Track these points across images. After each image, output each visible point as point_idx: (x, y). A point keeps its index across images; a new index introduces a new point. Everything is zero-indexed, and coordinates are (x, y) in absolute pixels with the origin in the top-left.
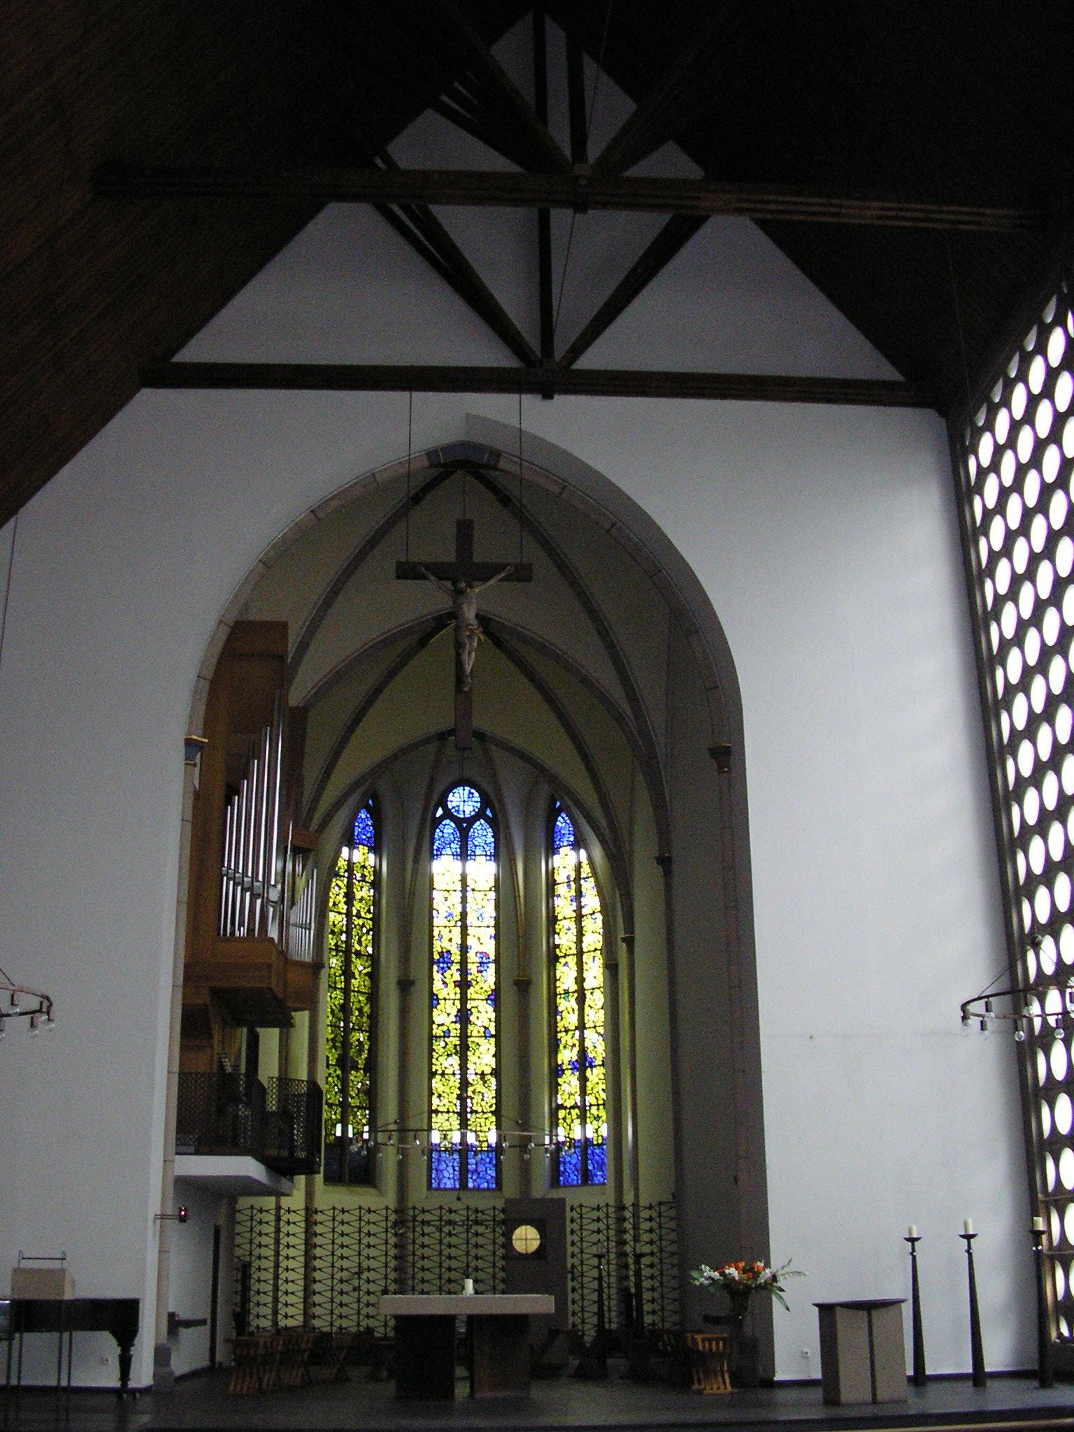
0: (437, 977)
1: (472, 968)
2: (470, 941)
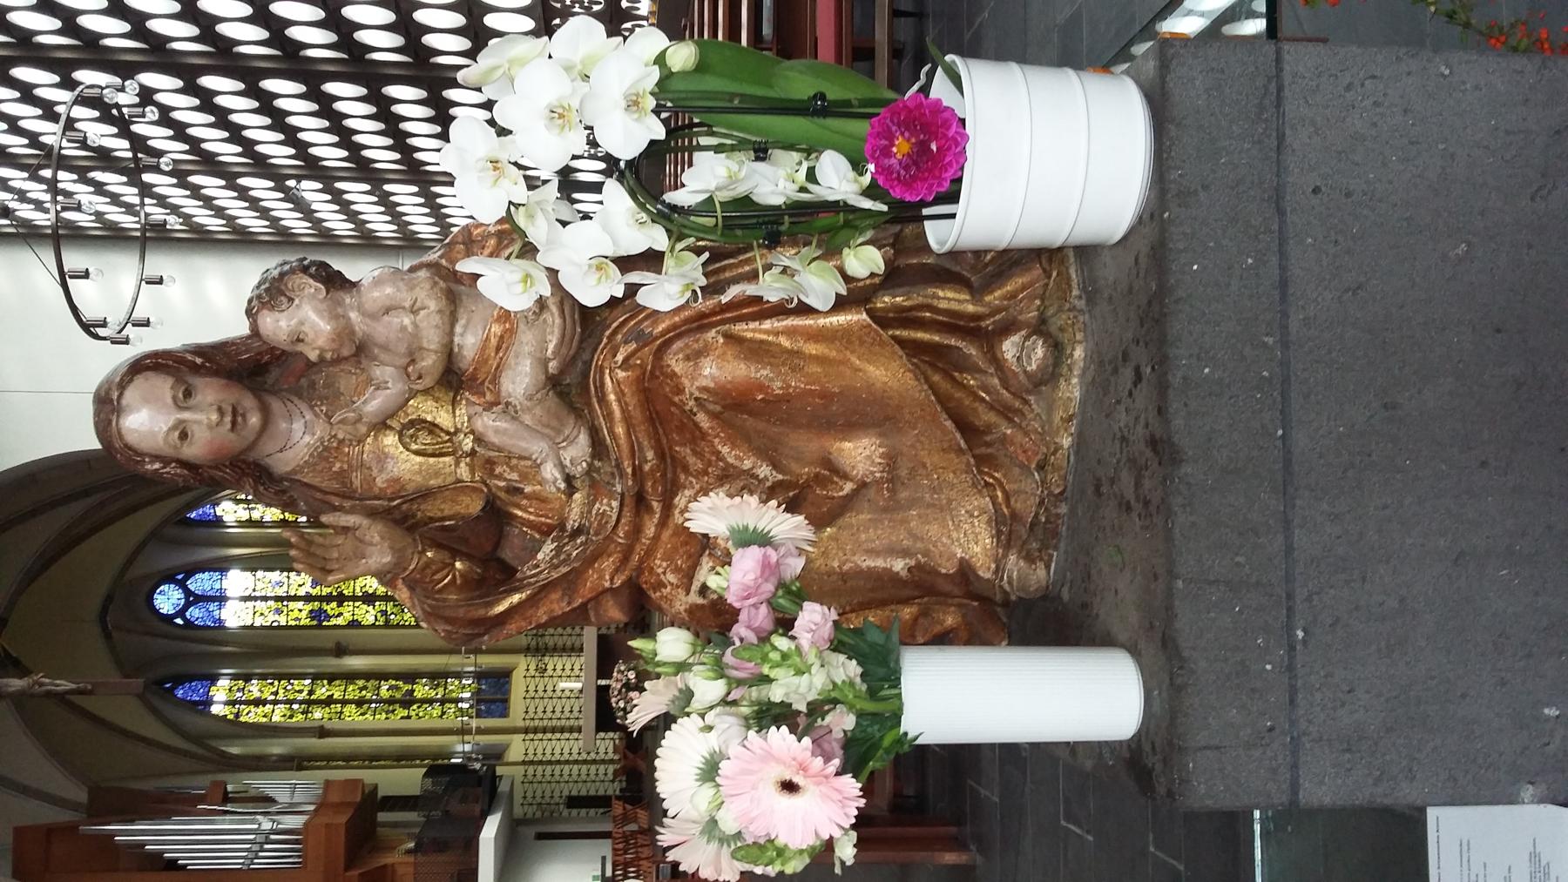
0: (334, 622)
1: (326, 591)
2: (301, 592)
